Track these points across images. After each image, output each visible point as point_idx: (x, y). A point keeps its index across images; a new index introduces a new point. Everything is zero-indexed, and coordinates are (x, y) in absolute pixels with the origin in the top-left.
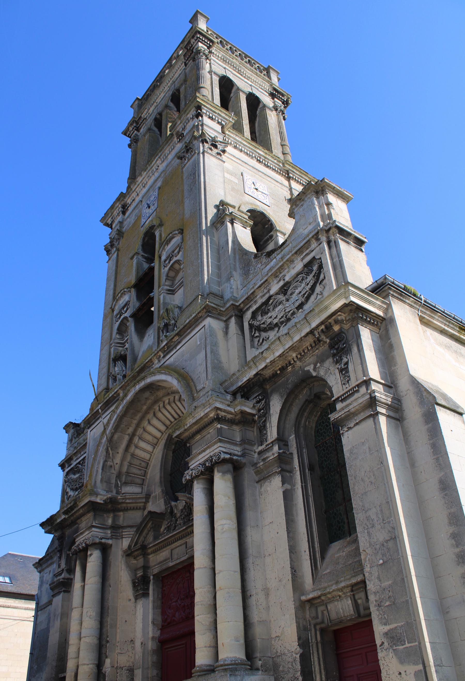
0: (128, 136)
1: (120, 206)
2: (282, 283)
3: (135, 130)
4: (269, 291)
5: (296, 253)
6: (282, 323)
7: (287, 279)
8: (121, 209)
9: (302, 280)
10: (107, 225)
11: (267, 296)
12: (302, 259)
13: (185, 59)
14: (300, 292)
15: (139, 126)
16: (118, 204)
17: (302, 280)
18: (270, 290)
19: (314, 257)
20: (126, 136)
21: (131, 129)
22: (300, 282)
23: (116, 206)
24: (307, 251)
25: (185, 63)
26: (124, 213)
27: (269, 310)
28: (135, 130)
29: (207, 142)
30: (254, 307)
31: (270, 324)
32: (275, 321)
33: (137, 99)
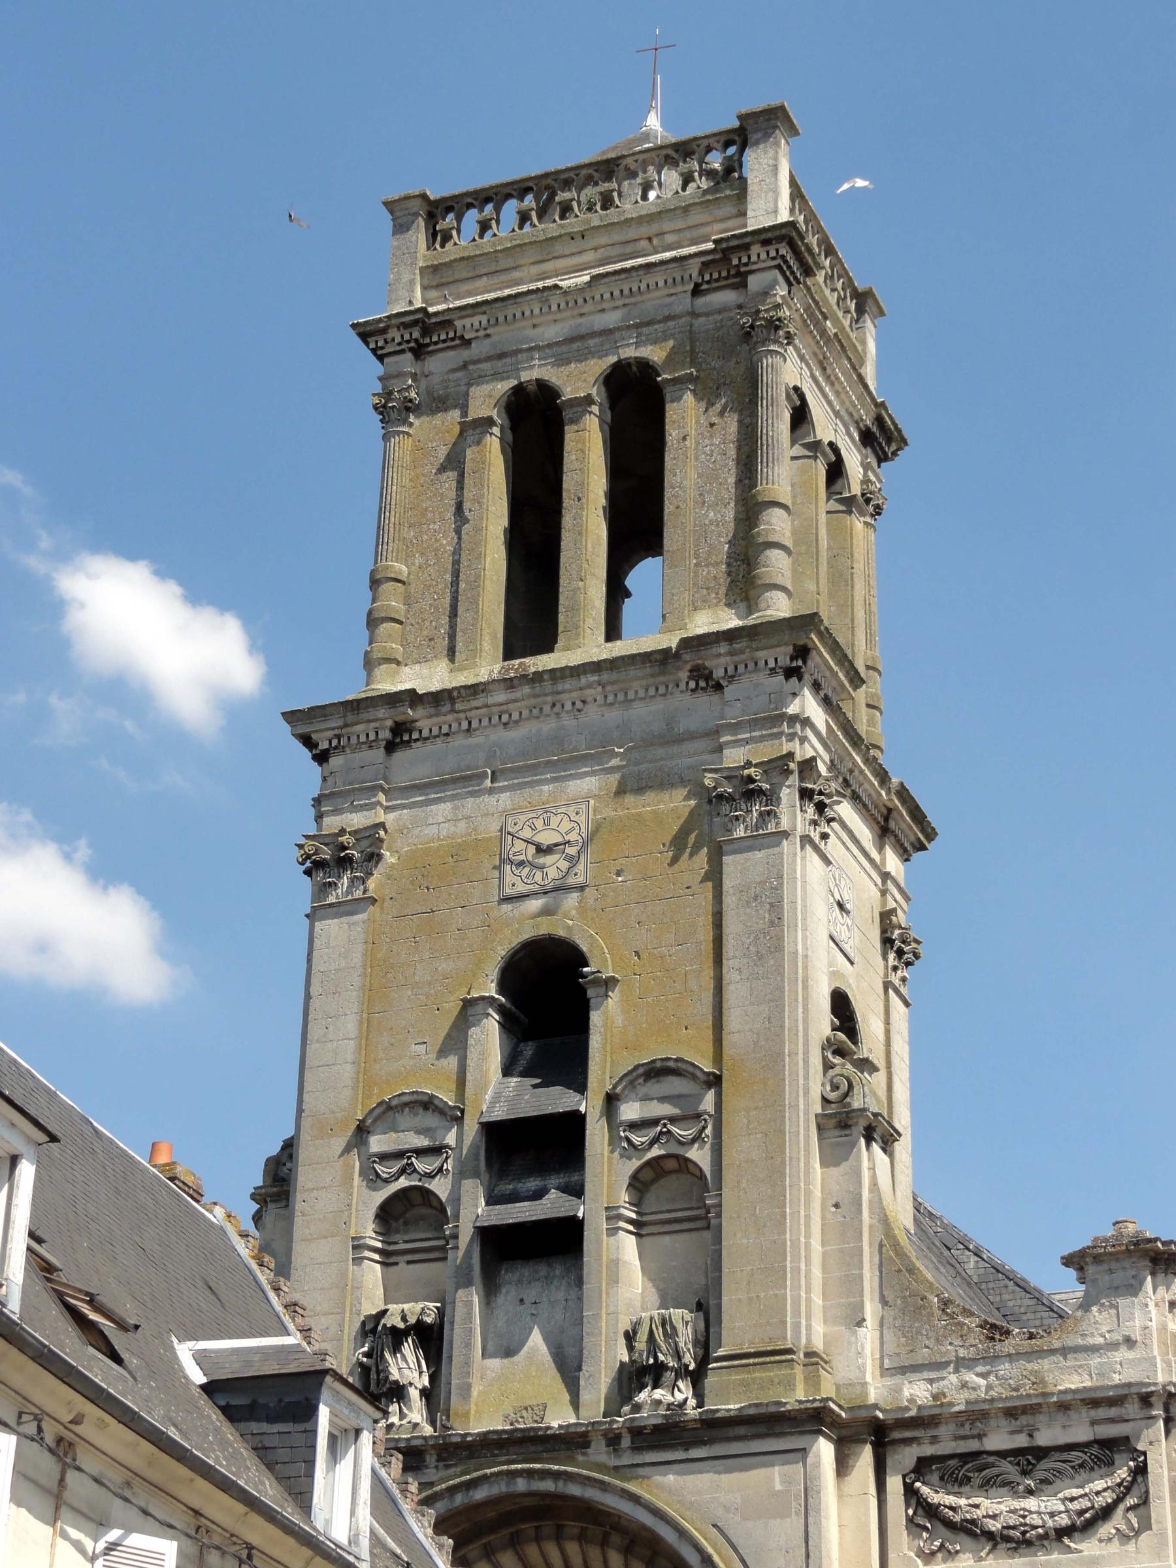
0: (374, 351)
1: (389, 723)
2: (1021, 1441)
3: (411, 349)
4: (980, 1437)
5: (1082, 1400)
6: (1008, 1539)
7: (1044, 1439)
8: (386, 734)
9: (1081, 1466)
10: (307, 741)
11: (973, 1446)
12: (1093, 1423)
13: (701, 273)
14: (1072, 1499)
15: (428, 345)
16: (381, 712)
17: (1081, 1466)
18: (985, 1435)
19: (1127, 1439)
20: (367, 344)
21: (394, 334)
22: (1073, 1467)
23: (372, 714)
24: (1113, 1412)
25: (697, 285)
26: (390, 747)
27: (969, 1479)
28: (411, 349)
29: (811, 799)
30: (928, 1450)
31: (973, 1522)
32: (994, 1526)
33: (424, 196)
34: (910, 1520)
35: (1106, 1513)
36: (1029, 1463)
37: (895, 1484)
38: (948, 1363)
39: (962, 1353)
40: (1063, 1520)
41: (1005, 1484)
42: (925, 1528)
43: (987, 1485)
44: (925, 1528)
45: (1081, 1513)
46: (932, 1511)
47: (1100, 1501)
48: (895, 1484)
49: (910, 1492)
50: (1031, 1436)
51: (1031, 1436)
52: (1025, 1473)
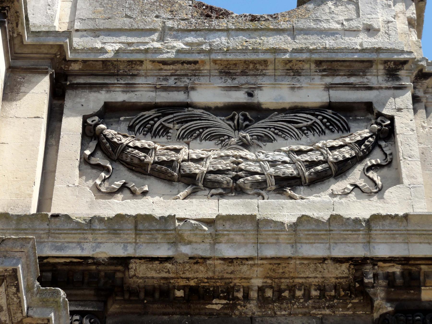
2: (240, 97)
4: (186, 90)
5: (319, 63)
11: (178, 97)
12: (329, 87)
14: (300, 152)
17: (310, 128)
18: (193, 89)
22: (300, 129)
30: (119, 96)
31: (170, 163)
34: (85, 161)
35: (342, 168)
36: (246, 118)
37: (72, 126)
38: (152, 31)
39: (170, 24)
40: (290, 170)
41: (211, 137)
42: (106, 170)
43: (187, 136)
44: (106, 170)
45: (311, 164)
46: (115, 153)
47: (338, 155)
48: (72, 126)
49: (89, 133)
50: (250, 95)
51: (250, 95)
52: (238, 128)
